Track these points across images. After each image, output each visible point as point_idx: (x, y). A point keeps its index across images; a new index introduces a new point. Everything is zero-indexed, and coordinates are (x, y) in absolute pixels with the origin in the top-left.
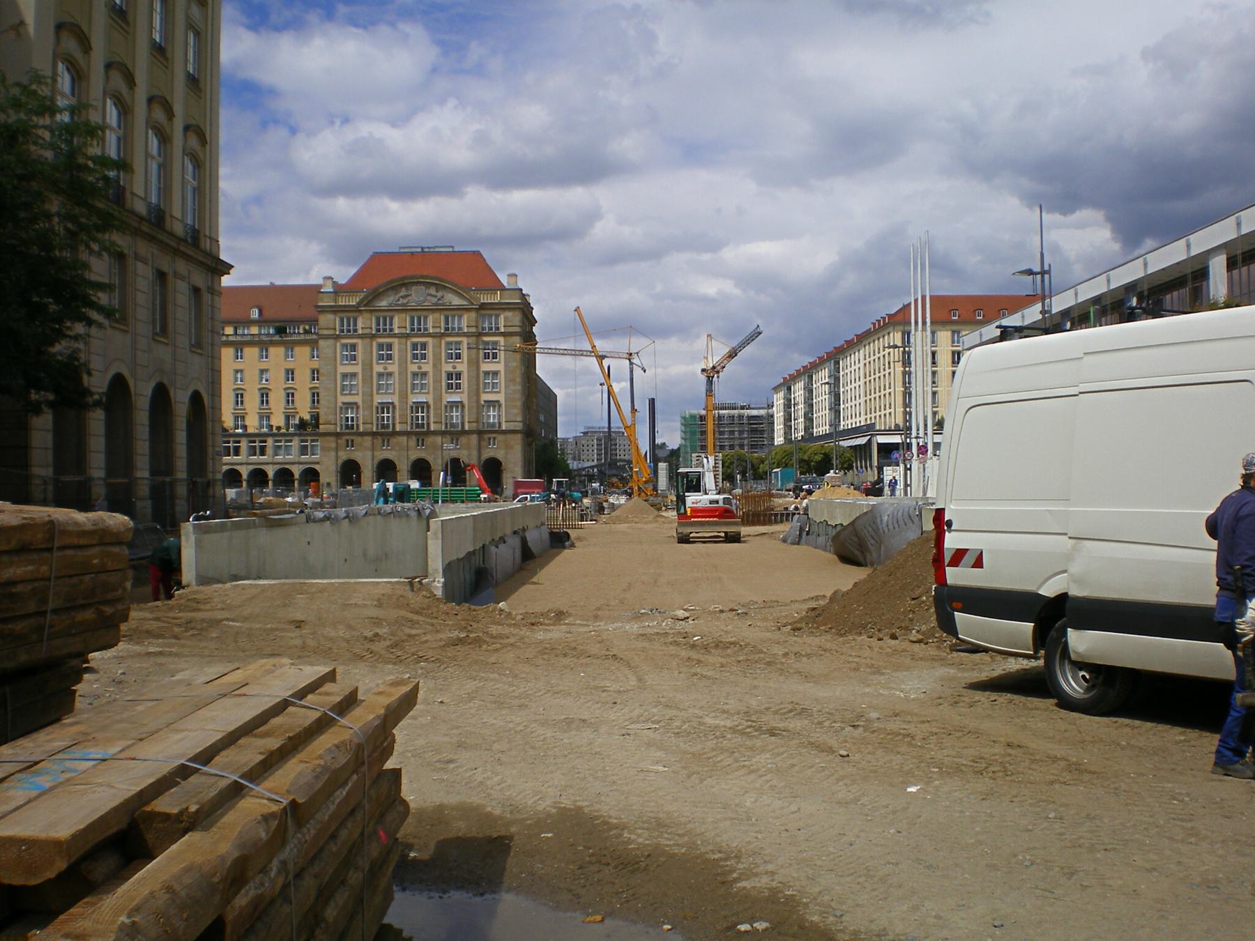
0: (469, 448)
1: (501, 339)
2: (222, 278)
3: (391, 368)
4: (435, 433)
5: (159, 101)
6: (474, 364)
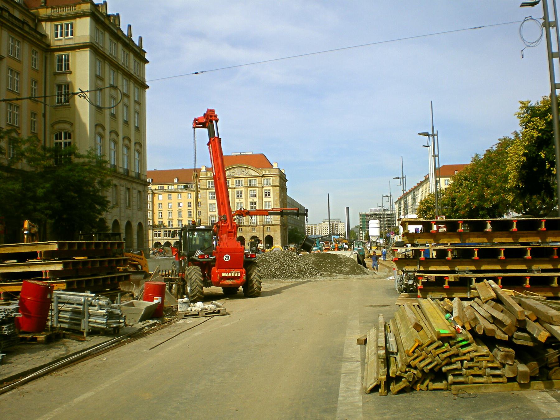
0: (259, 231)
1: (271, 188)
4: (246, 226)
5: (127, 138)
6: (261, 198)
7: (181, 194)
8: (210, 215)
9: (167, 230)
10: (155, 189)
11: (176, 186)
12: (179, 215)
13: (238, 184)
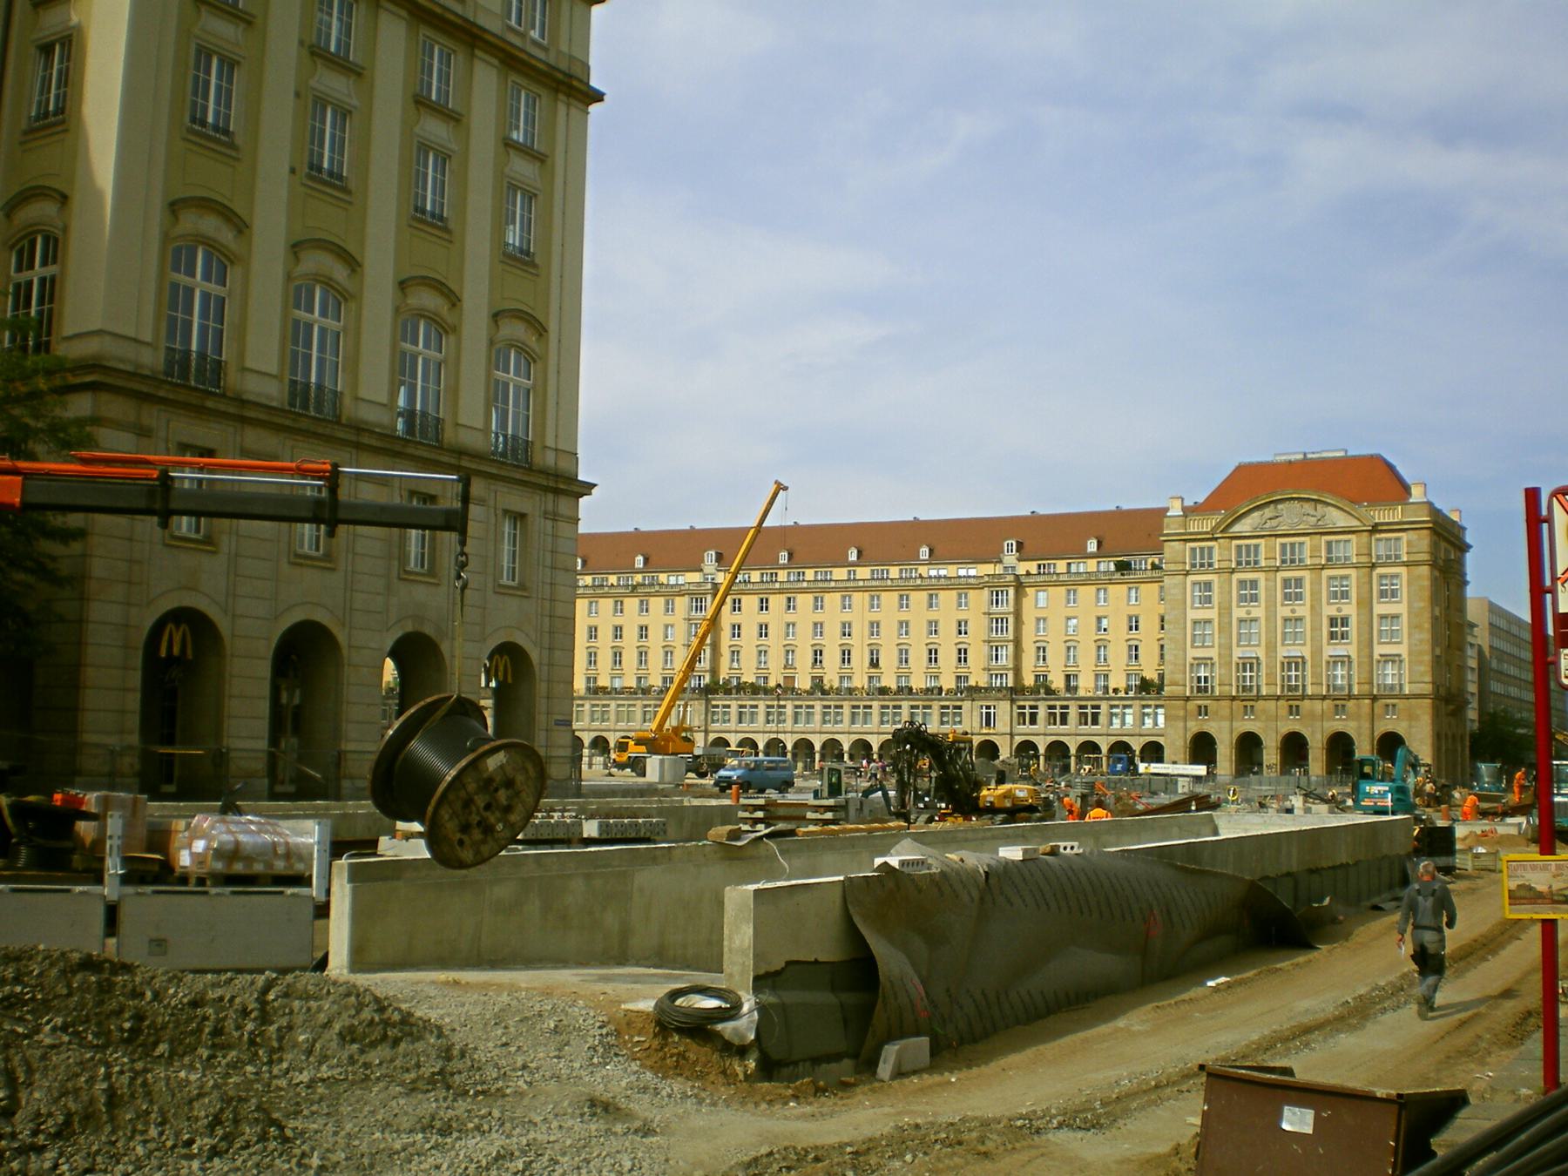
0: (1358, 717)
1: (1402, 570)
2: (581, 500)
3: (1256, 613)
4: (1311, 698)
6: (1366, 604)
7: (1105, 590)
8: (1194, 659)
9: (1058, 703)
10: (1028, 574)
11: (1091, 565)
12: (1099, 656)
13: (1288, 557)
